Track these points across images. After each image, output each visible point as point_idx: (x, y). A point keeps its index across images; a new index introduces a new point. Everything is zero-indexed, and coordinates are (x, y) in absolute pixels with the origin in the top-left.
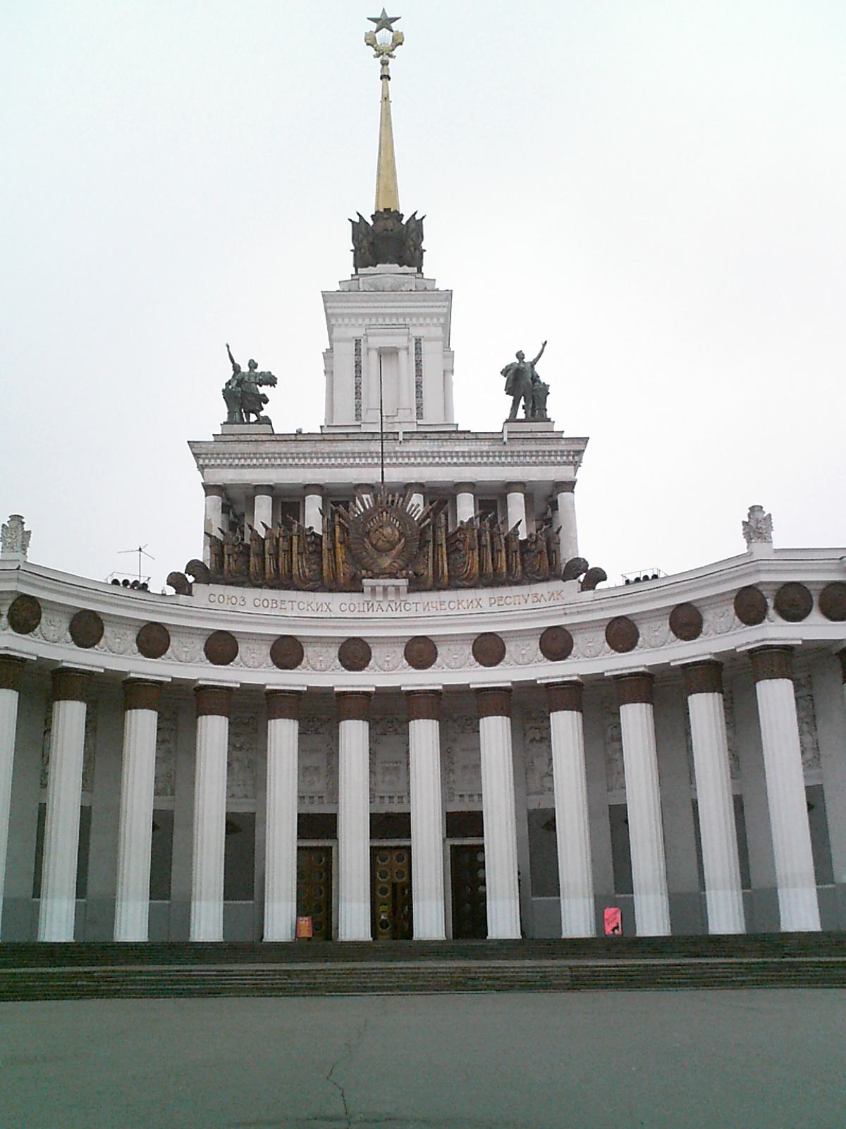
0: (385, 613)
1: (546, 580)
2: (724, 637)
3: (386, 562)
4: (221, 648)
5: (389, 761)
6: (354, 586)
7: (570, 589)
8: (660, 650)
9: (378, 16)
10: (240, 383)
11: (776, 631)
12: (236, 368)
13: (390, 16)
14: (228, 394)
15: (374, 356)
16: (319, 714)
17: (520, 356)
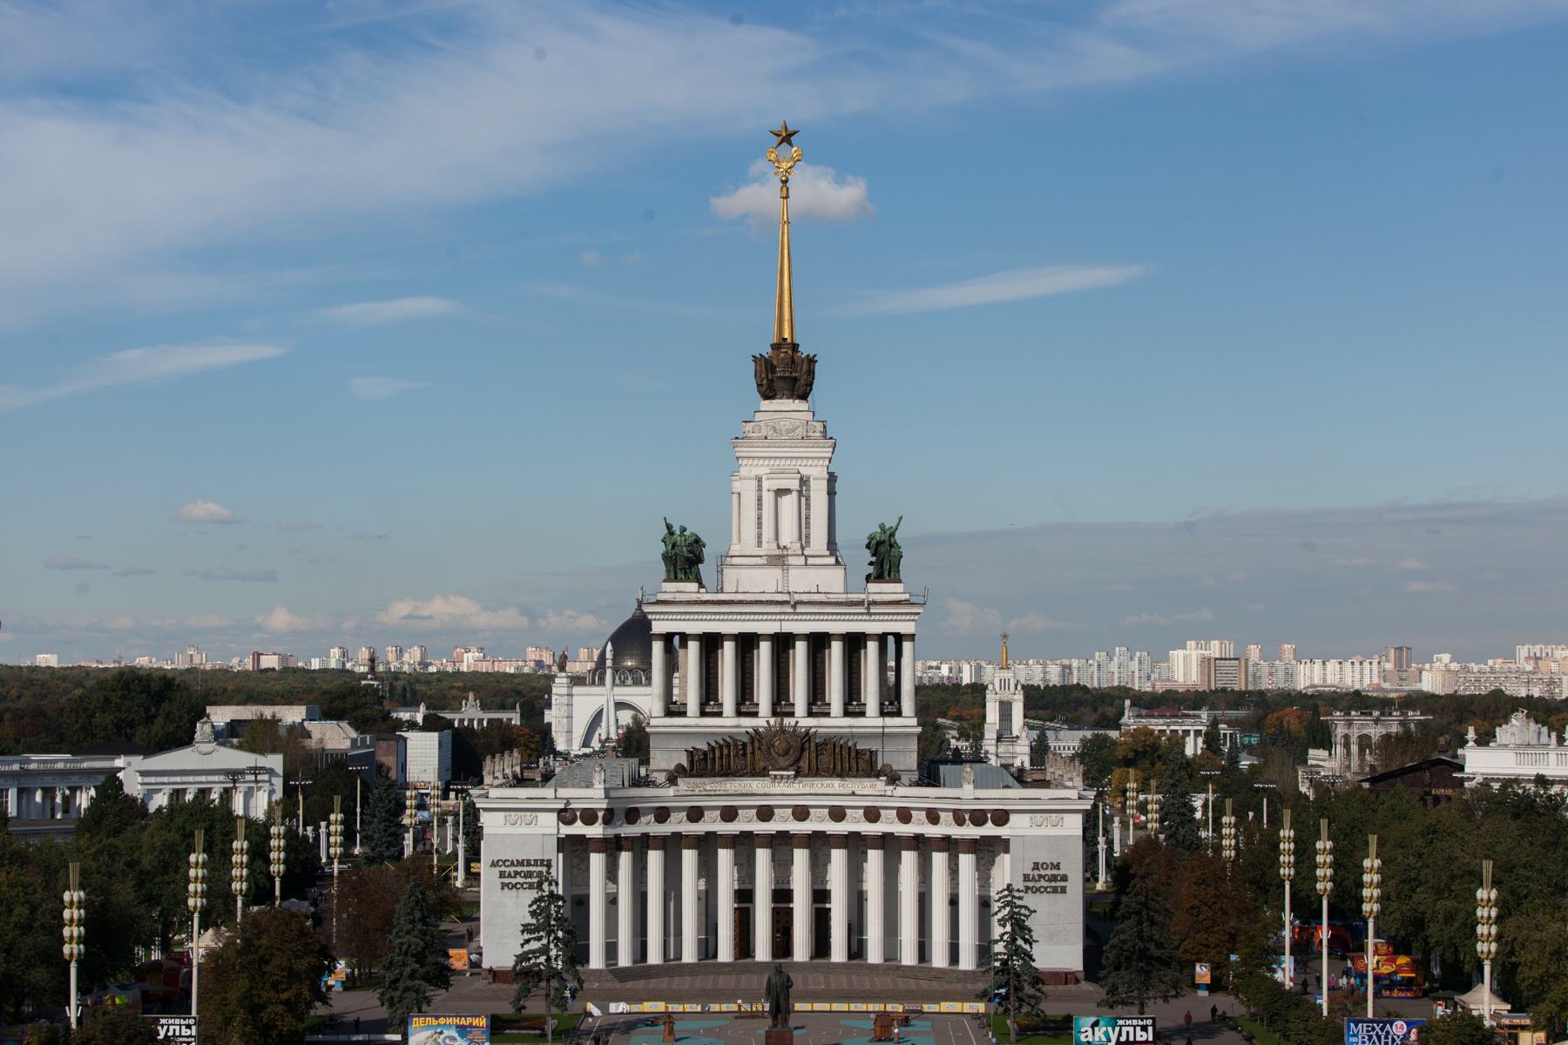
0: (781, 789)
1: (869, 776)
2: (946, 828)
3: (782, 761)
4: (695, 814)
5: (782, 866)
6: (763, 773)
7: (880, 785)
8: (919, 826)
9: (778, 128)
10: (674, 546)
11: (970, 831)
12: (669, 527)
13: (791, 129)
14: (666, 557)
15: (772, 495)
16: (744, 844)
17: (882, 527)
